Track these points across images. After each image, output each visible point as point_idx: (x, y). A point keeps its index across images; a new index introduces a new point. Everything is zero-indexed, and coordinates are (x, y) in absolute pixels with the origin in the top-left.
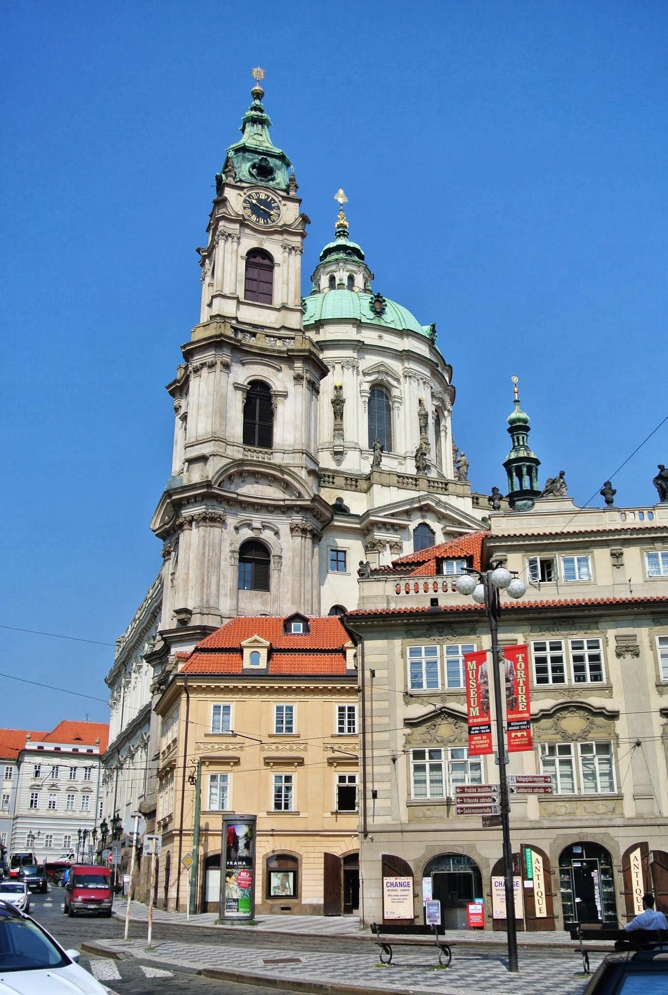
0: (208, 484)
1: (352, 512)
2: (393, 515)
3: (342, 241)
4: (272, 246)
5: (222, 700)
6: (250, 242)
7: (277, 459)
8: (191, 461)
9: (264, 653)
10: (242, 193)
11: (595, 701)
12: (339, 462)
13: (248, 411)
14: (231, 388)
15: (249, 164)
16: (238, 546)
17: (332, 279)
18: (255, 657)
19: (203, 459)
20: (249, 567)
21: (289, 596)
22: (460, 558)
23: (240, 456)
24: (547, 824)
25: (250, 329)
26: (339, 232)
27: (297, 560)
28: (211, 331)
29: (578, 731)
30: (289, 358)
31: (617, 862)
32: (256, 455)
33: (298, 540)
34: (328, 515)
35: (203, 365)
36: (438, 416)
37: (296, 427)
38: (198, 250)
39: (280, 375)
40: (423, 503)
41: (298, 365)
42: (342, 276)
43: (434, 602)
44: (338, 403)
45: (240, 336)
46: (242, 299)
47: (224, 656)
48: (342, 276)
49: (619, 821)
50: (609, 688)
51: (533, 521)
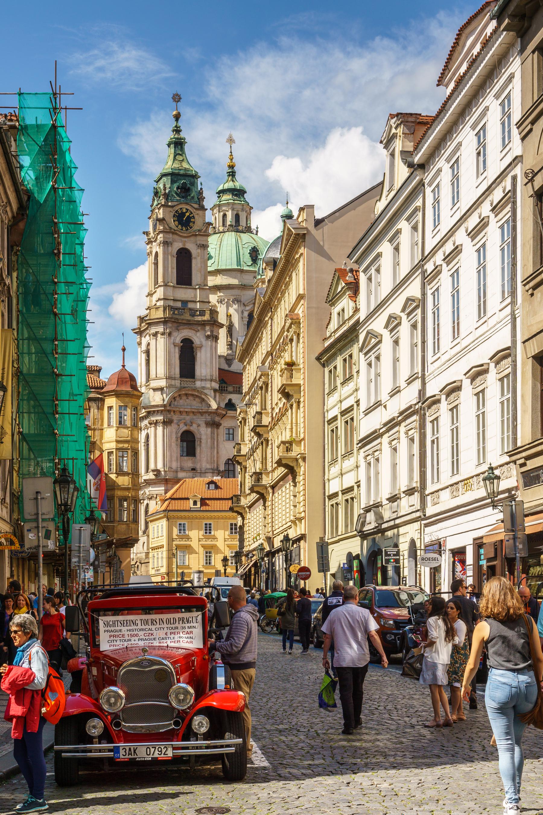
0: (165, 406)
3: (229, 185)
4: (191, 246)
7: (198, 384)
10: (171, 209)
12: (230, 365)
14: (172, 346)
16: (180, 435)
17: (225, 216)
18: (195, 503)
19: (161, 389)
21: (205, 459)
26: (229, 172)
27: (209, 440)
32: (187, 383)
38: (144, 233)
39: (198, 334)
41: (208, 328)
46: (176, 285)
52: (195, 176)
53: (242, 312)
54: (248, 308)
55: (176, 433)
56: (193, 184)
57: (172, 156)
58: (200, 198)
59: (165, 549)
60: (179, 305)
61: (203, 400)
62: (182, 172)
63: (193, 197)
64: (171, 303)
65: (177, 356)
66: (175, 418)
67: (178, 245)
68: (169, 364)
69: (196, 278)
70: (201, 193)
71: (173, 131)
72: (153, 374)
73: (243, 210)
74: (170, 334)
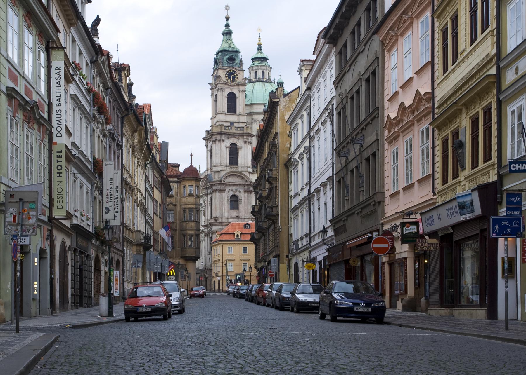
3: (259, 55)
4: (235, 91)
5: (230, 246)
8: (215, 172)
9: (240, 235)
13: (230, 154)
15: (227, 57)
17: (256, 73)
18: (238, 236)
19: (219, 172)
23: (228, 170)
30: (242, 135)
33: (246, 194)
37: (244, 159)
38: (209, 84)
39: (240, 141)
41: (245, 137)
45: (227, 128)
52: (238, 52)
56: (237, 56)
57: (225, 40)
58: (241, 64)
59: (221, 261)
60: (229, 124)
62: (230, 49)
63: (237, 64)
64: (224, 124)
65: (228, 153)
67: (228, 91)
70: (241, 61)
71: (225, 26)
72: (214, 164)
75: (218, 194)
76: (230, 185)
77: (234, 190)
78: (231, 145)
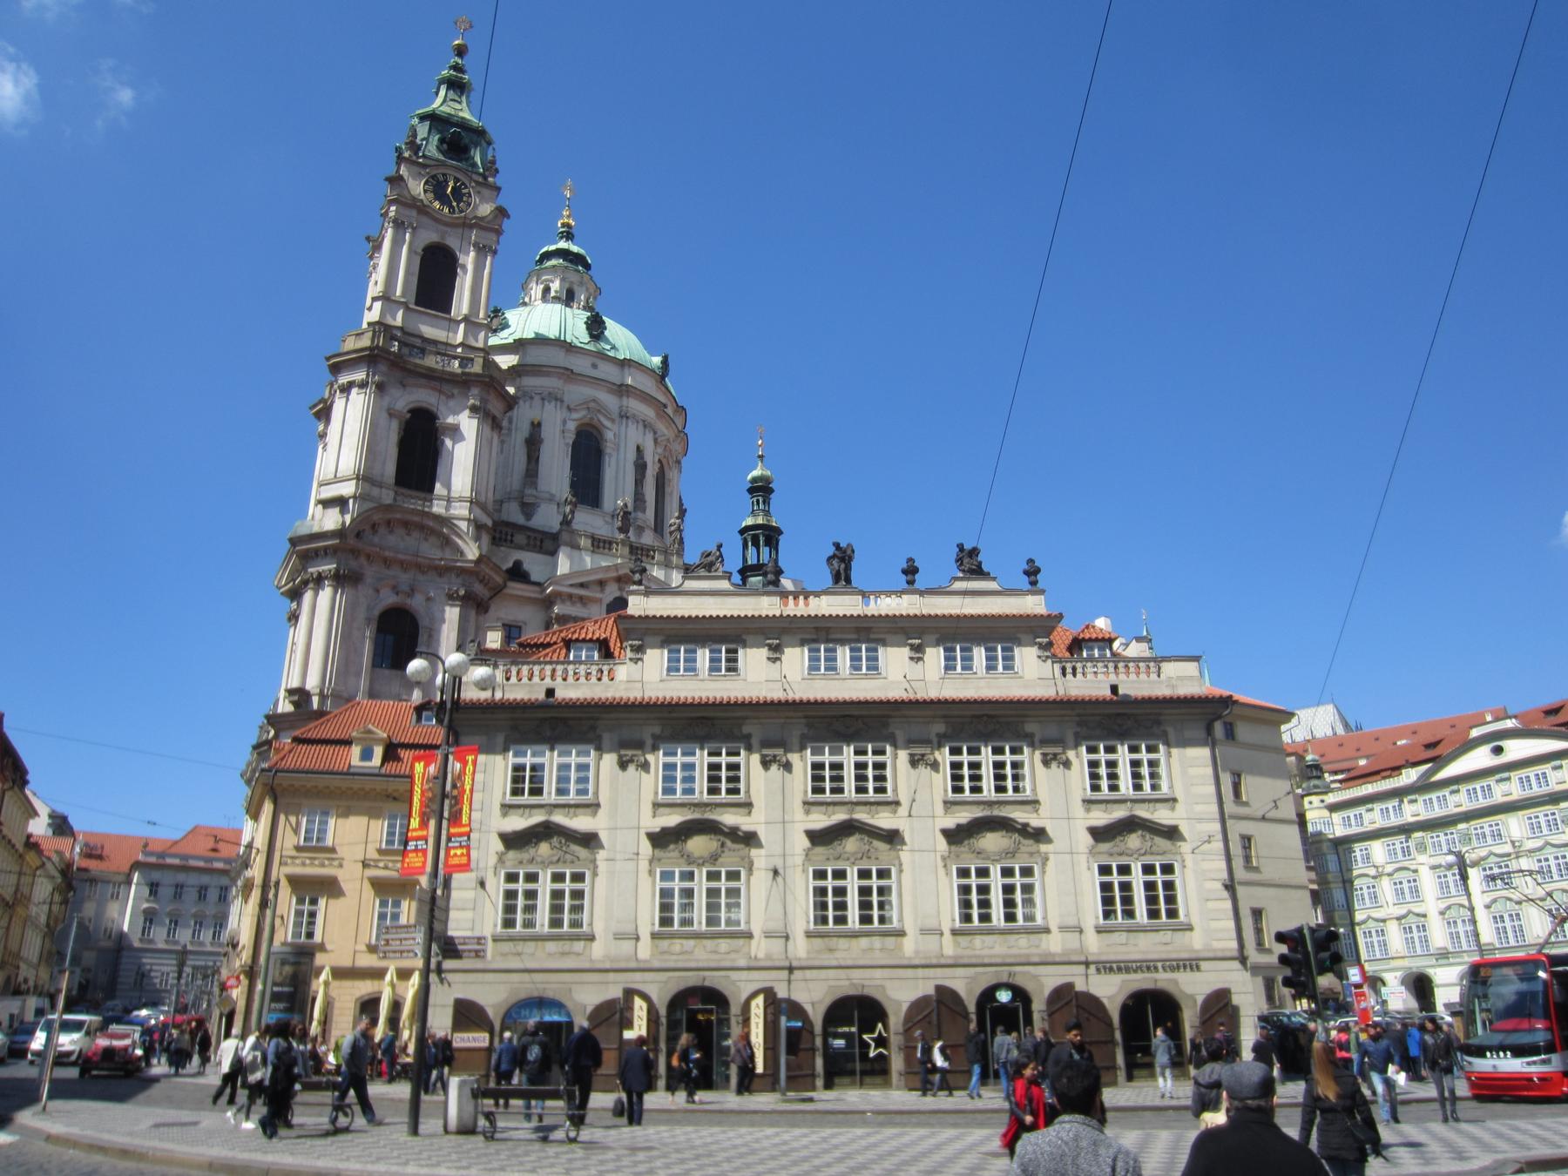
0: (340, 533)
1: (534, 578)
2: (582, 585)
3: (563, 245)
6: (430, 236)
7: (438, 508)
8: (326, 503)
11: (729, 818)
12: (529, 516)
14: (385, 415)
16: (377, 613)
17: (547, 290)
18: (367, 755)
19: (340, 502)
20: (390, 638)
22: (591, 640)
24: (656, 964)
25: (418, 342)
28: (366, 342)
29: (706, 854)
30: (464, 382)
31: (735, 1009)
34: (499, 579)
35: (351, 385)
36: (662, 469)
39: (452, 403)
40: (622, 572)
41: (475, 391)
42: (555, 286)
43: (550, 692)
44: (533, 443)
46: (412, 306)
47: (329, 749)
48: (555, 286)
49: (742, 963)
50: (748, 805)
51: (679, 600)
53: (564, 422)
54: (575, 416)
55: (369, 608)
61: (447, 542)
65: (394, 438)
66: (370, 572)
68: (371, 449)
69: (462, 303)
73: (581, 284)
74: (380, 387)
75: (326, 594)
76: (387, 562)
77: (405, 588)
78: (411, 411)
